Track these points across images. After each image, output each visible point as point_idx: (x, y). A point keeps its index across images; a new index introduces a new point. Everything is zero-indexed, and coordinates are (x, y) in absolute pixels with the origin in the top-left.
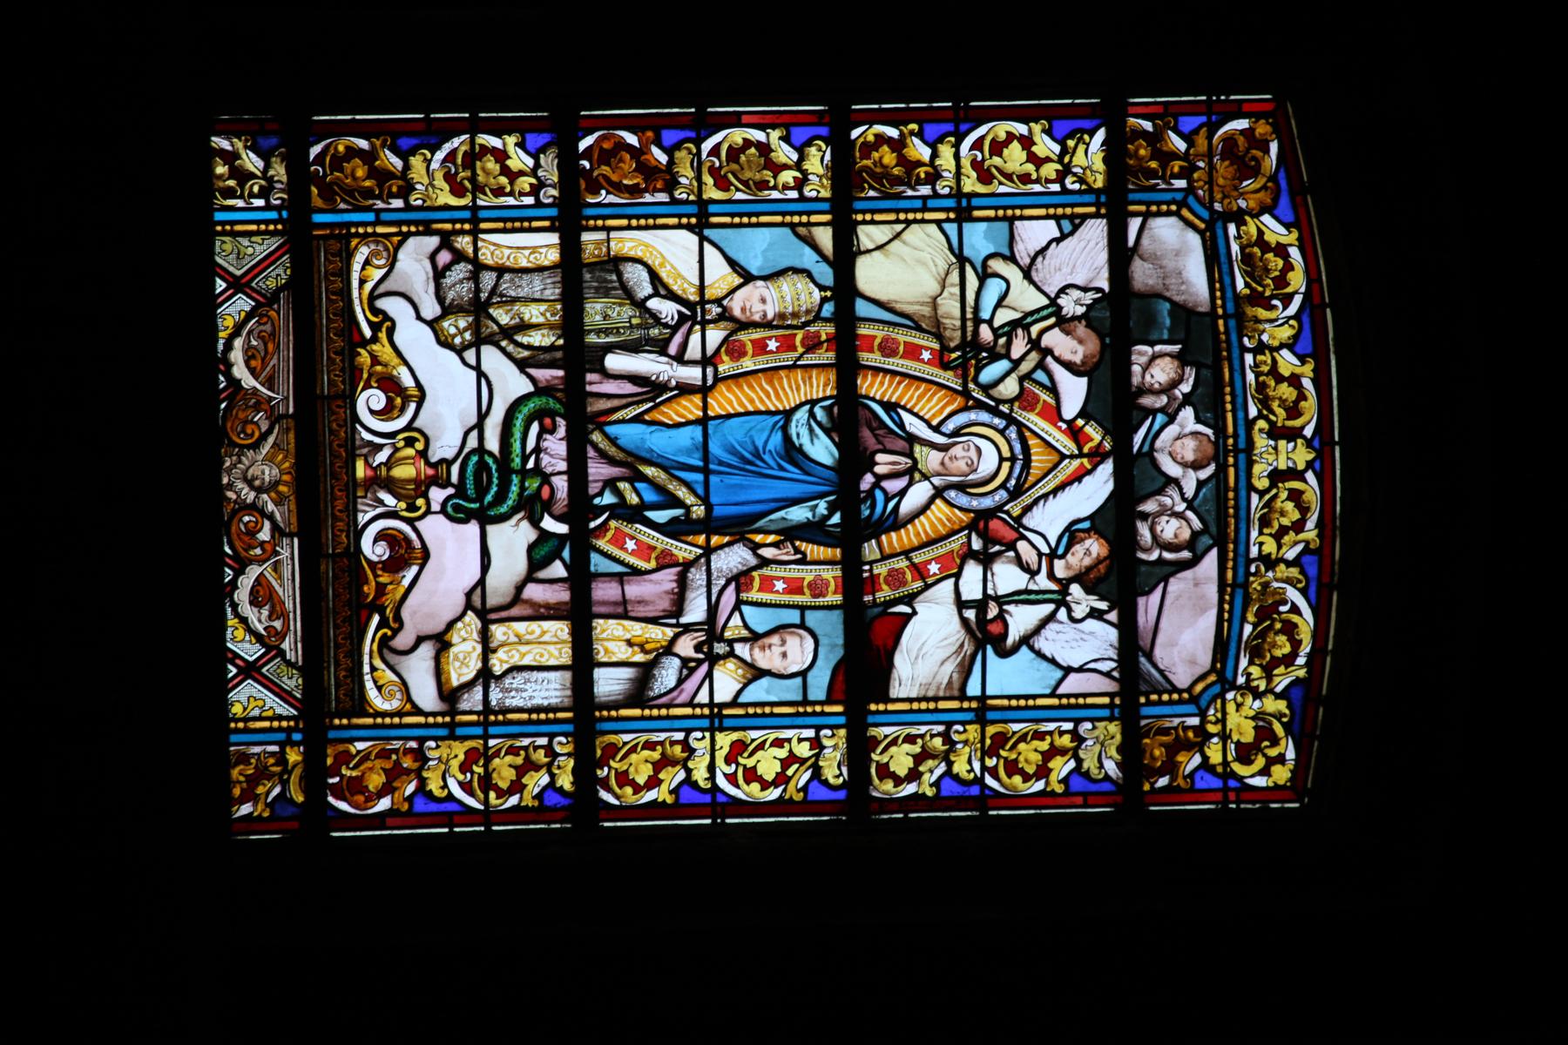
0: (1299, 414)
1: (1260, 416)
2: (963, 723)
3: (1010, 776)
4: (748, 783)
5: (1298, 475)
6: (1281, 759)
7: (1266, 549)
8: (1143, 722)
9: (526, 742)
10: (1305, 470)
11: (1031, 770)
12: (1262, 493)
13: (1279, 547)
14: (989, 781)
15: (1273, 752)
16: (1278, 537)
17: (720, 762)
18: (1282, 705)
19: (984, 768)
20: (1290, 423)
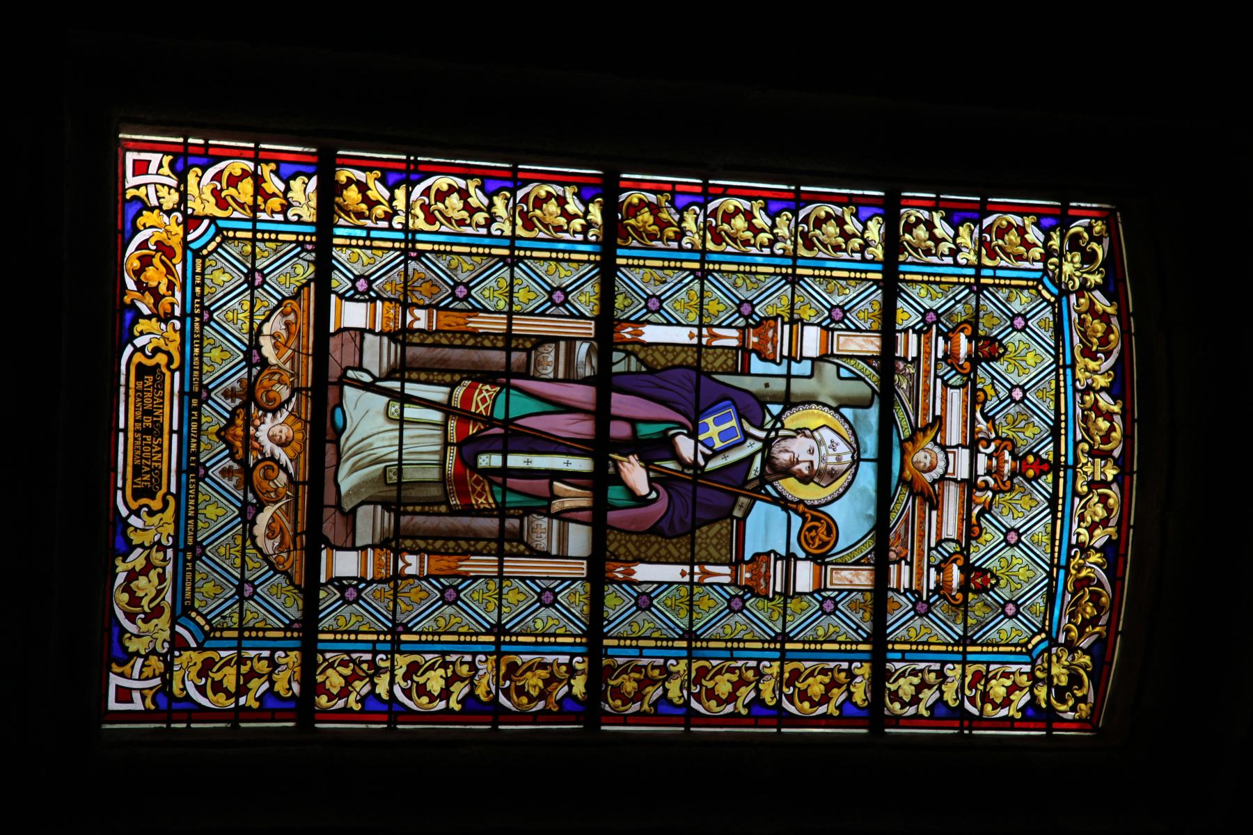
1: (1083, 440)
4: (801, 702)
5: (1105, 484)
6: (1084, 699)
7: (1082, 538)
8: (605, 662)
12: (1082, 498)
13: (1091, 537)
15: (1079, 694)
17: (399, 679)
18: (1086, 659)
19: (690, 693)
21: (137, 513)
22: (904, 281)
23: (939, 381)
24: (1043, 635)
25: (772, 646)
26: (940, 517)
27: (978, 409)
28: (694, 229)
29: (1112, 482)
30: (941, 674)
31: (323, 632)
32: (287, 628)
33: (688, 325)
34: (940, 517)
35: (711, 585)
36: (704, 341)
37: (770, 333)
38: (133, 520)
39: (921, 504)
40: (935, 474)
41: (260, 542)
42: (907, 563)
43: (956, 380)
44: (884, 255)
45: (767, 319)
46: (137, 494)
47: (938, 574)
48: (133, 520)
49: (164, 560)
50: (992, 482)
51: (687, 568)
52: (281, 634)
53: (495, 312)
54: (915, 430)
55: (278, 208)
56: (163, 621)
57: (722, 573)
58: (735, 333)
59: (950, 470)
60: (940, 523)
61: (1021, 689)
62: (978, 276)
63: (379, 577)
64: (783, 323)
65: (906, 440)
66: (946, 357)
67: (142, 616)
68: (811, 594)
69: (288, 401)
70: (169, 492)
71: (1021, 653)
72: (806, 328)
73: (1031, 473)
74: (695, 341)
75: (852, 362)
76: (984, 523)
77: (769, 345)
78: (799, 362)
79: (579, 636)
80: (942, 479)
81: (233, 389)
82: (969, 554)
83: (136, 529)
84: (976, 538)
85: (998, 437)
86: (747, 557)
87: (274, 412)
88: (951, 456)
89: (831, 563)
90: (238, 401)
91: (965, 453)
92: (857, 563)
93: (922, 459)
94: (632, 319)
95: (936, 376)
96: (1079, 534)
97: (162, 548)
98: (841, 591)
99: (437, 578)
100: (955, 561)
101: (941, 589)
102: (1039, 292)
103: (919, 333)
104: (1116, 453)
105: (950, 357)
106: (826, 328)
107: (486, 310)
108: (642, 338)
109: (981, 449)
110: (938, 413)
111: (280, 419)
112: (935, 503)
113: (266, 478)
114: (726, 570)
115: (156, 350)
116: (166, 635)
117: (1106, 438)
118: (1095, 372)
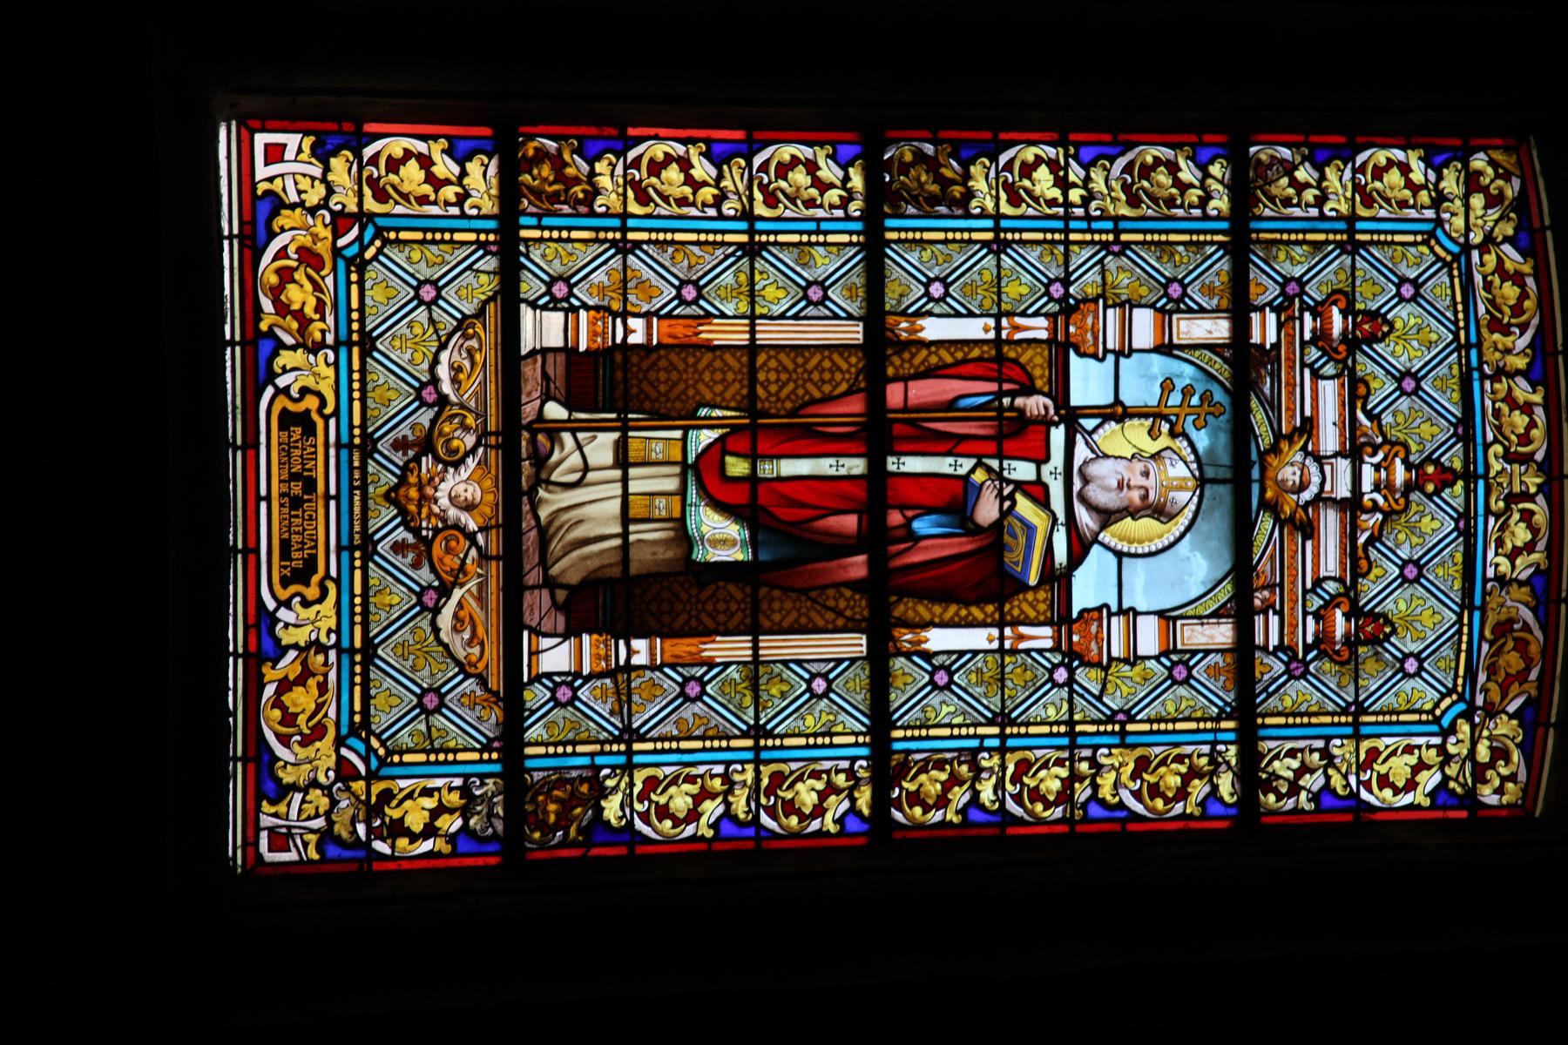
0: (1530, 442)
1: (1496, 441)
2: (1110, 747)
3: (1152, 799)
5: (1527, 496)
6: (1513, 778)
7: (1502, 569)
9: (701, 769)
10: (1536, 494)
11: (1401, 784)
12: (1497, 516)
13: (1513, 567)
14: (765, 819)
15: (1504, 771)
16: (1512, 556)
20: (1520, 449)
21: (287, 604)
22: (1258, 241)
23: (1307, 372)
24: (1455, 697)
25: (1109, 728)
26: (1316, 549)
27: (1359, 405)
28: (986, 189)
29: (1536, 494)
30: (1326, 753)
31: (530, 744)
32: (486, 748)
33: (981, 316)
34: (1316, 549)
35: (1027, 652)
36: (1004, 335)
37: (1090, 320)
38: (283, 614)
39: (1290, 533)
40: (1306, 496)
41: (443, 635)
42: (1275, 613)
43: (1329, 369)
44: (1231, 209)
45: (1085, 300)
46: (285, 583)
47: (1317, 623)
48: (283, 614)
49: (326, 664)
50: (1381, 501)
51: (995, 632)
52: (476, 756)
53: (735, 317)
54: (1278, 436)
55: (453, 199)
56: (326, 745)
57: (1042, 636)
58: (1042, 322)
59: (1328, 487)
60: (1316, 555)
61: (1429, 767)
62: (1351, 231)
63: (598, 669)
64: (1106, 307)
65: (1267, 452)
66: (1314, 341)
67: (298, 738)
68: (1157, 658)
69: (473, 451)
70: (327, 576)
71: (1427, 723)
72: (1136, 311)
73: (1430, 488)
74: (992, 335)
75: (1197, 353)
76: (1373, 554)
77: (1089, 336)
78: (1128, 356)
79: (861, 733)
80: (1318, 498)
81: (405, 437)
82: (1357, 595)
83: (287, 625)
84: (1364, 576)
85: (1386, 441)
86: (1075, 615)
87: (457, 465)
88: (1327, 468)
89: (1182, 617)
90: (411, 453)
91: (1344, 465)
92: (1216, 614)
93: (1291, 477)
94: (911, 310)
95: (1303, 365)
96: (1497, 565)
97: (322, 649)
98: (1194, 653)
99: (673, 667)
100: (1338, 606)
101: (1322, 642)
102: (1432, 249)
103: (1277, 310)
104: (1539, 457)
105: (1321, 337)
106: (1162, 311)
107: (723, 315)
108: (922, 335)
109: (1367, 459)
110: (1308, 413)
111: (464, 474)
112: (1309, 530)
113: (448, 550)
114: (1047, 631)
115: (304, 391)
116: (332, 762)
117: (1525, 439)
118: (1508, 351)
